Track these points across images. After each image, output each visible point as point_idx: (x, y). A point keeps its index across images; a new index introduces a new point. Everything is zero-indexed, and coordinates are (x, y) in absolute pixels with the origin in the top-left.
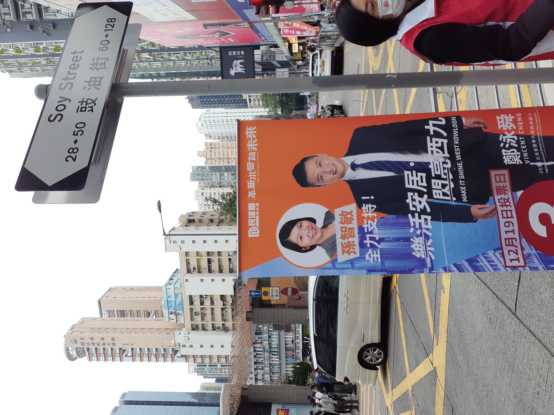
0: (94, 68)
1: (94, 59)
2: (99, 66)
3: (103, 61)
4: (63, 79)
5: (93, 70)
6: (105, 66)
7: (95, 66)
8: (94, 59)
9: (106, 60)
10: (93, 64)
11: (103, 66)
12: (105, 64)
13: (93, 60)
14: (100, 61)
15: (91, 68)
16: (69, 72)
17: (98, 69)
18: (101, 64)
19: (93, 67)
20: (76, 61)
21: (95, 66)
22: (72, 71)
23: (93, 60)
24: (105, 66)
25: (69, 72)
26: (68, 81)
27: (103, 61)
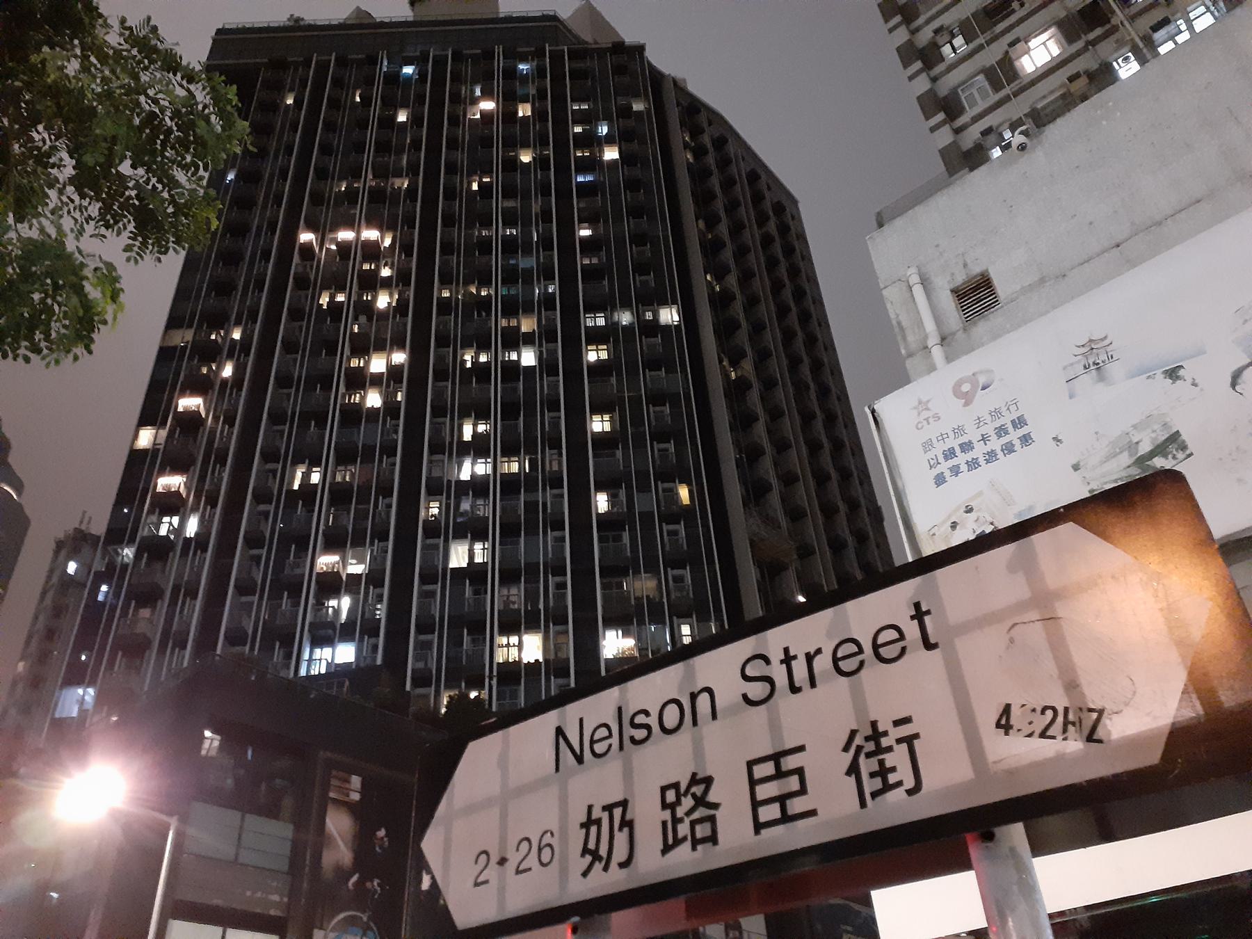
0: (859, 748)
1: (907, 720)
2: (867, 766)
3: (904, 774)
4: (786, 650)
5: (846, 749)
6: (874, 795)
7: (870, 746)
8: (907, 720)
9: (909, 783)
10: (876, 735)
11: (878, 783)
12: (887, 787)
13: (897, 723)
14: (897, 757)
15: (853, 733)
16: (819, 651)
17: (853, 769)
18: (883, 772)
19: (858, 740)
20: (876, 647)
21: (870, 746)
22: (823, 663)
23: (897, 723)
24: (874, 795)
25: (819, 651)
26: (779, 673)
27: (904, 774)
